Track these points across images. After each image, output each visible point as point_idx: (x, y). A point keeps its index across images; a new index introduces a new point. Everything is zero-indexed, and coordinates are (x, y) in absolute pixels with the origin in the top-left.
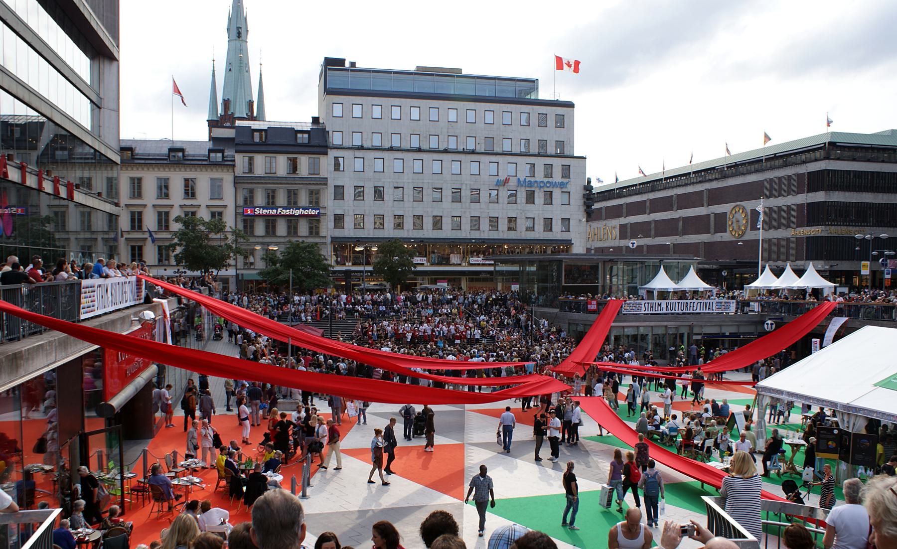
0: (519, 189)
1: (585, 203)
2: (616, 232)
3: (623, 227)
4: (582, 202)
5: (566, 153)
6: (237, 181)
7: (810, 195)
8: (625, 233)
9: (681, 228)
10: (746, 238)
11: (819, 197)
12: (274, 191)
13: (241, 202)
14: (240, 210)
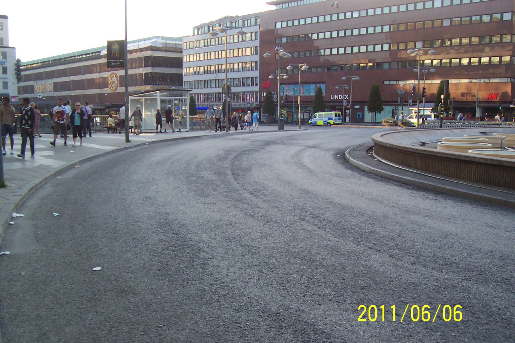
1: (16, 73)
2: (51, 88)
3: (55, 84)
4: (15, 72)
5: (5, 45)
7: (146, 68)
8: (57, 87)
9: (71, 87)
10: (117, 91)
11: (149, 70)
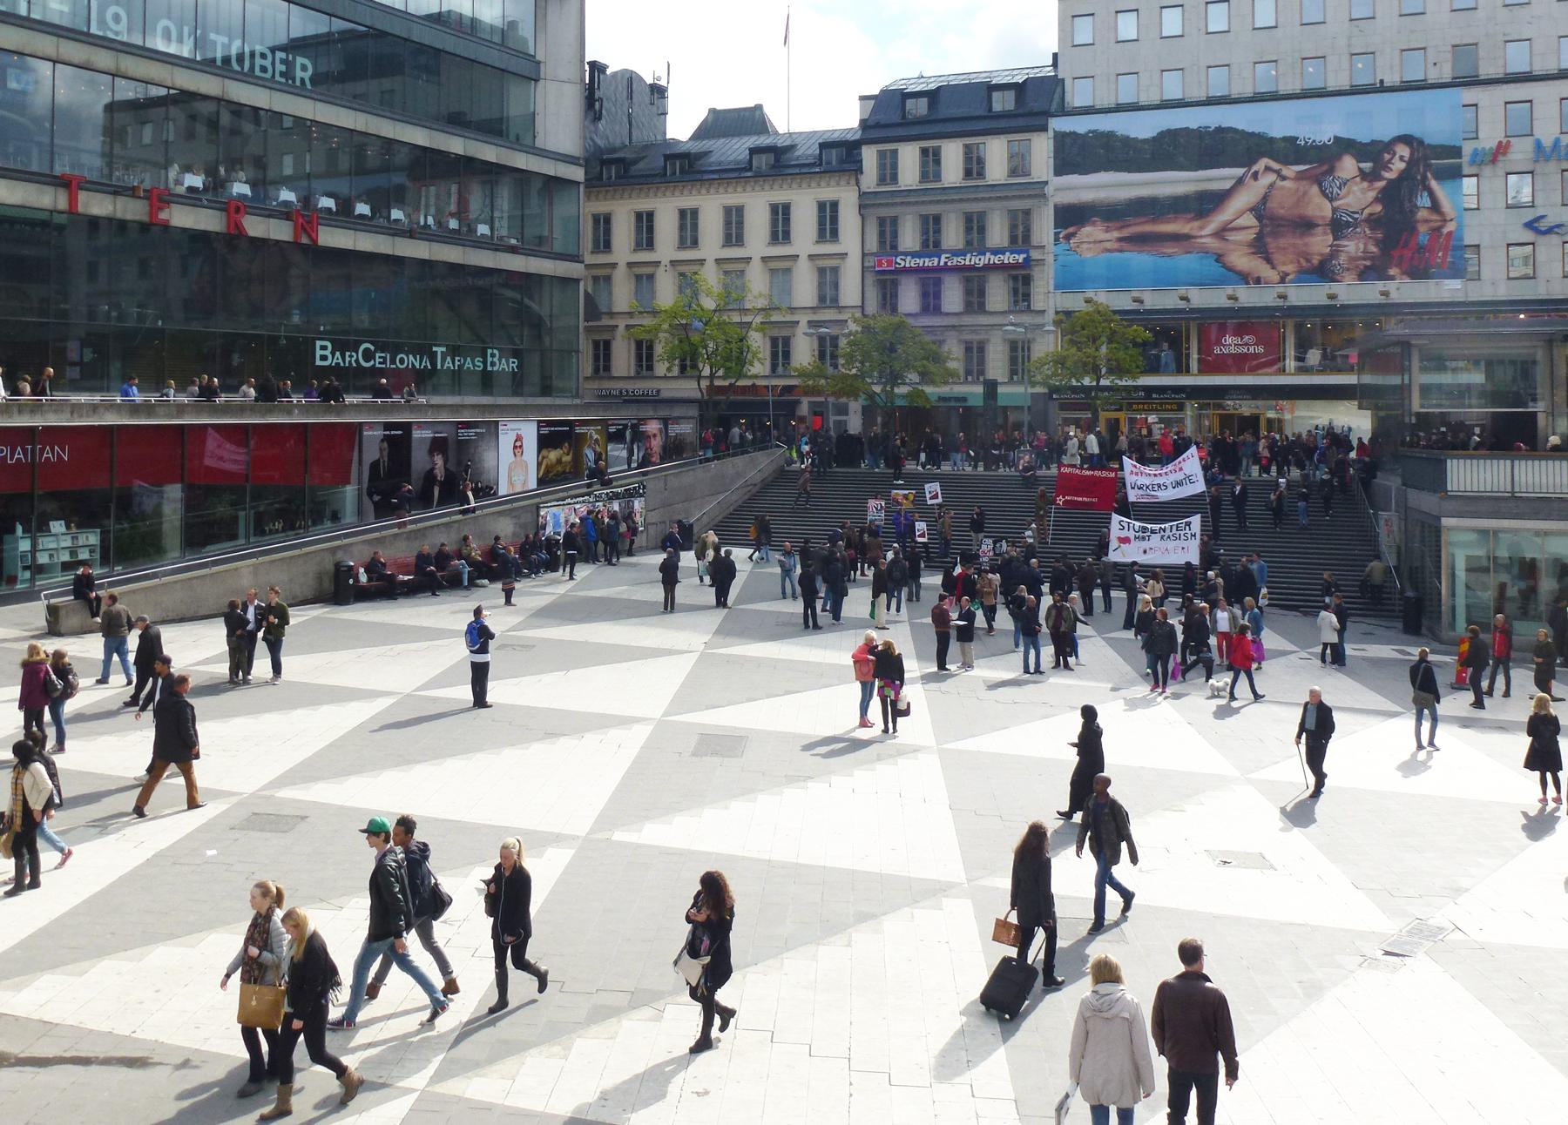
0: (1539, 168)
6: (866, 203)
12: (937, 219)
13: (873, 244)
14: (870, 262)
